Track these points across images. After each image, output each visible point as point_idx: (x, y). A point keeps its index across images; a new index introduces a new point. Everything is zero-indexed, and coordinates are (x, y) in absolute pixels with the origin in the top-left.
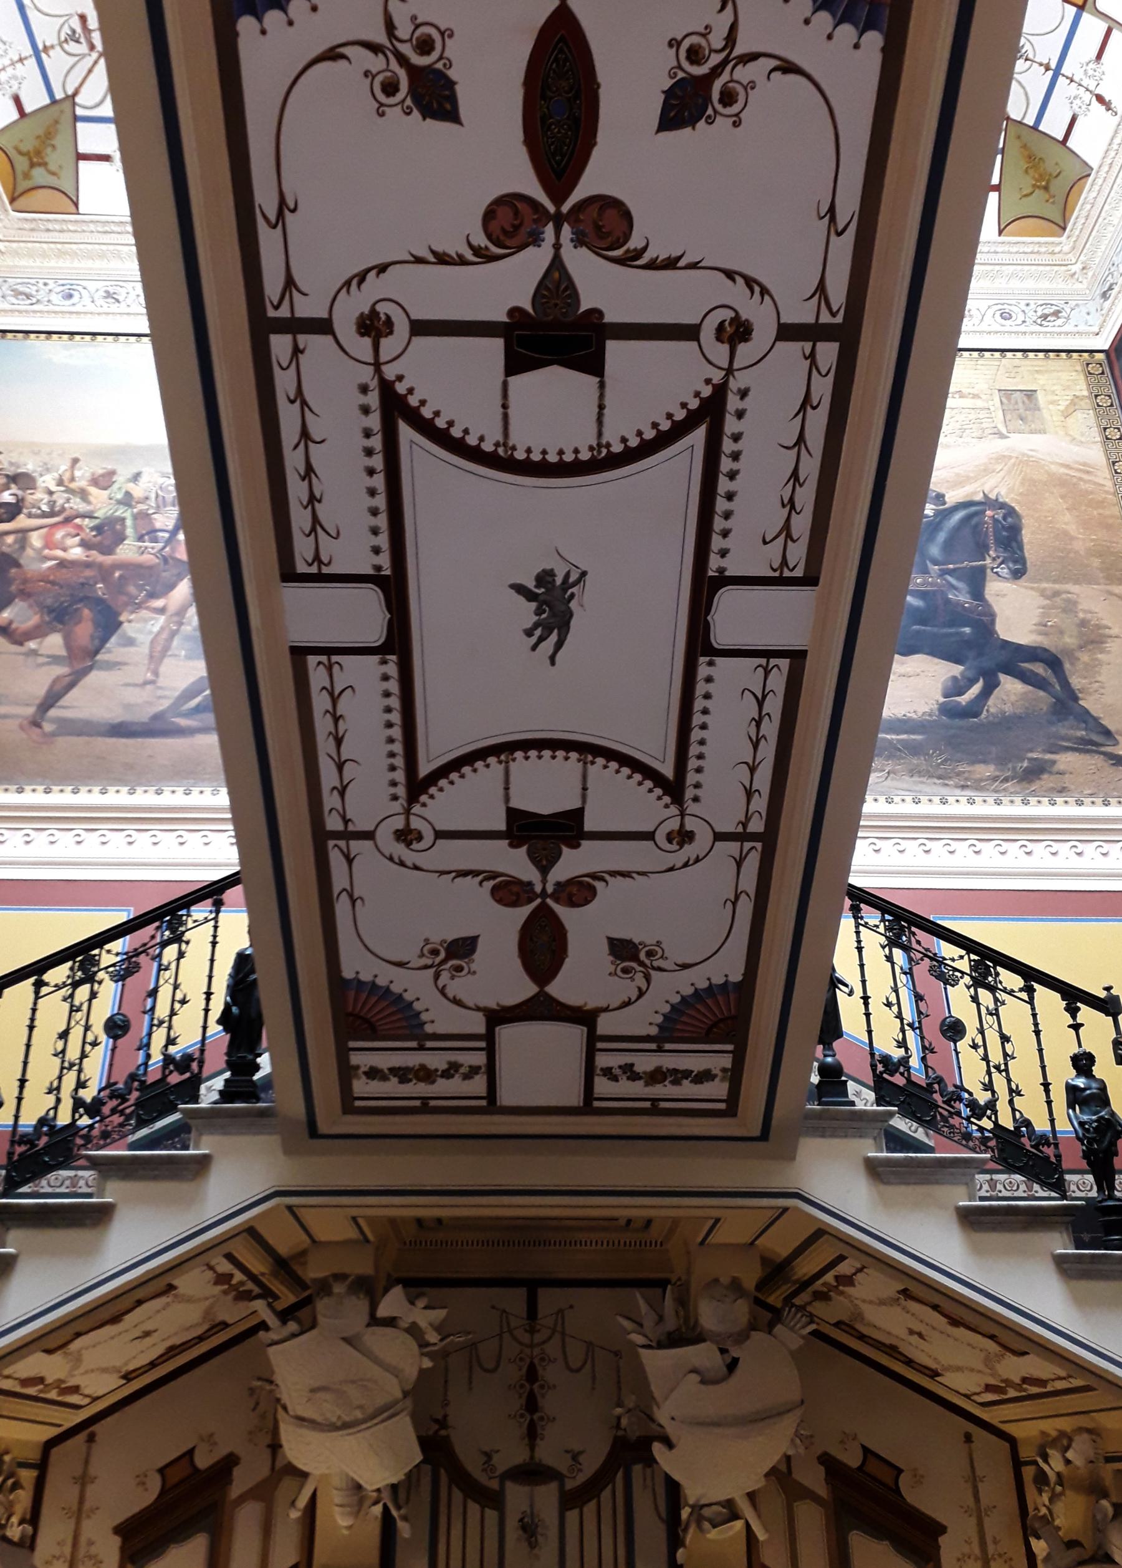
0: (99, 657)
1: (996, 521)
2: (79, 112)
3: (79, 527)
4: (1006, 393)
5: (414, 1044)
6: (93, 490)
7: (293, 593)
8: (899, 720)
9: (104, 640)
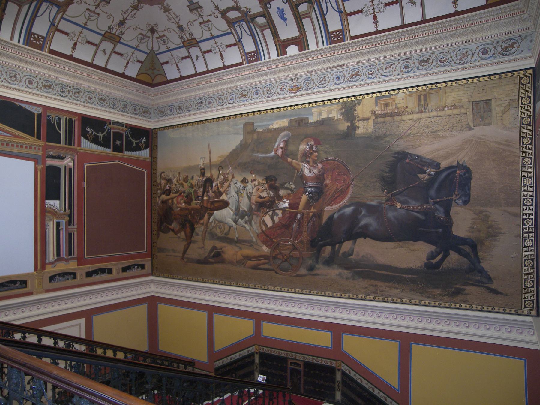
0: (192, 239)
1: (460, 175)
2: (156, 53)
3: (183, 196)
4: (476, 103)
6: (184, 183)
8: (409, 269)
9: (192, 234)
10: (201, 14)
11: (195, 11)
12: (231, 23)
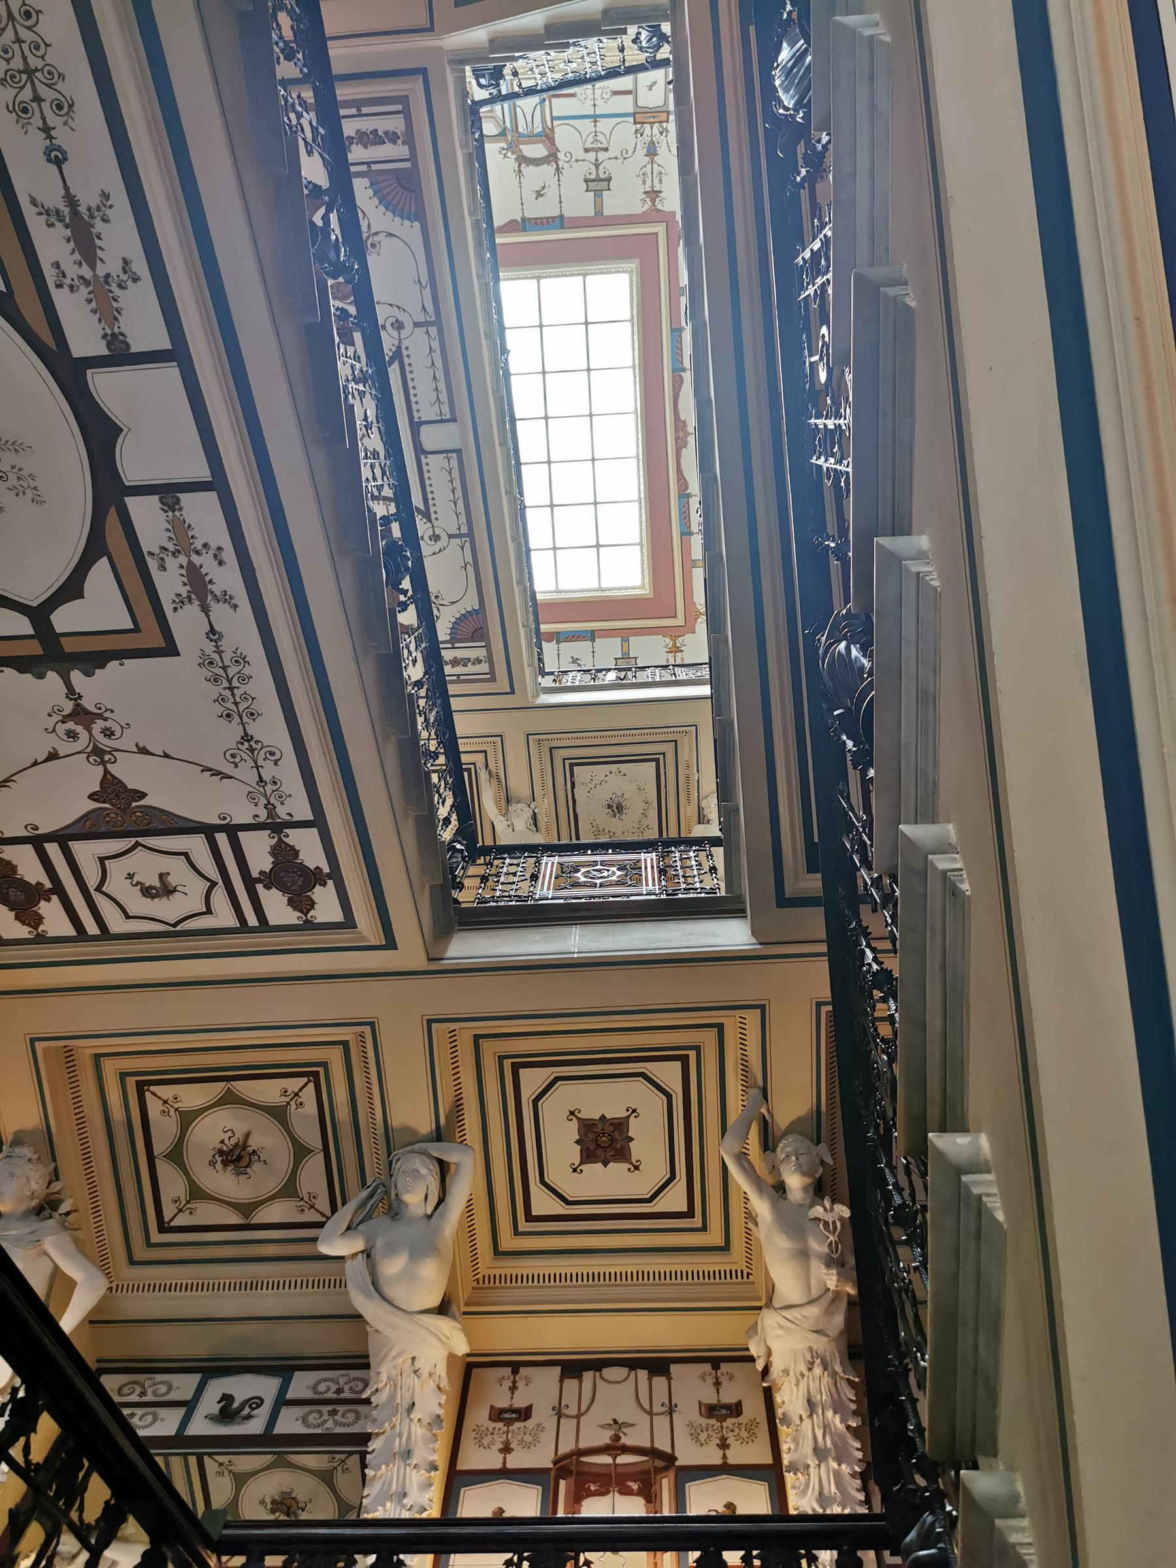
5: (374, 167)
7: (457, 446)
10: (593, 167)
11: (602, 176)
12: (548, 136)
